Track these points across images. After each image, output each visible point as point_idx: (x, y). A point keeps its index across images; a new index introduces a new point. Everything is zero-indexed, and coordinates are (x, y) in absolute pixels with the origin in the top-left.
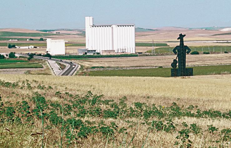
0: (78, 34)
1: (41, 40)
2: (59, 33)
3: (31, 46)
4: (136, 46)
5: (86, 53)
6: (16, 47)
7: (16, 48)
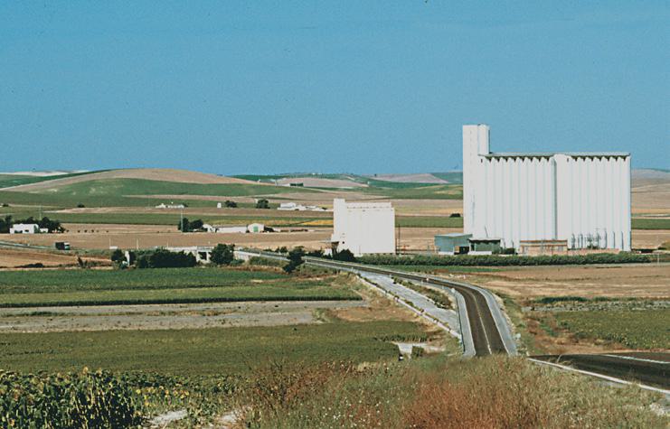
0: (361, 190)
1: (260, 207)
2: (301, 185)
3: (256, 225)
4: (632, 228)
5: (464, 250)
6: (205, 226)
7: (206, 230)
